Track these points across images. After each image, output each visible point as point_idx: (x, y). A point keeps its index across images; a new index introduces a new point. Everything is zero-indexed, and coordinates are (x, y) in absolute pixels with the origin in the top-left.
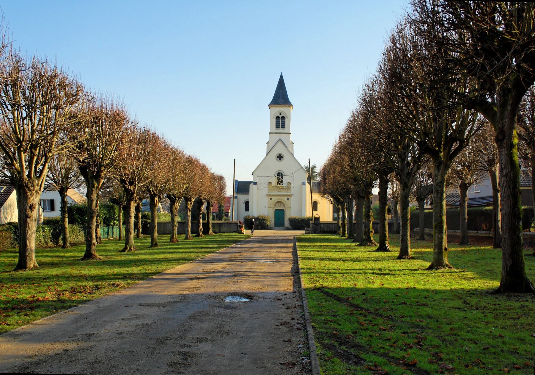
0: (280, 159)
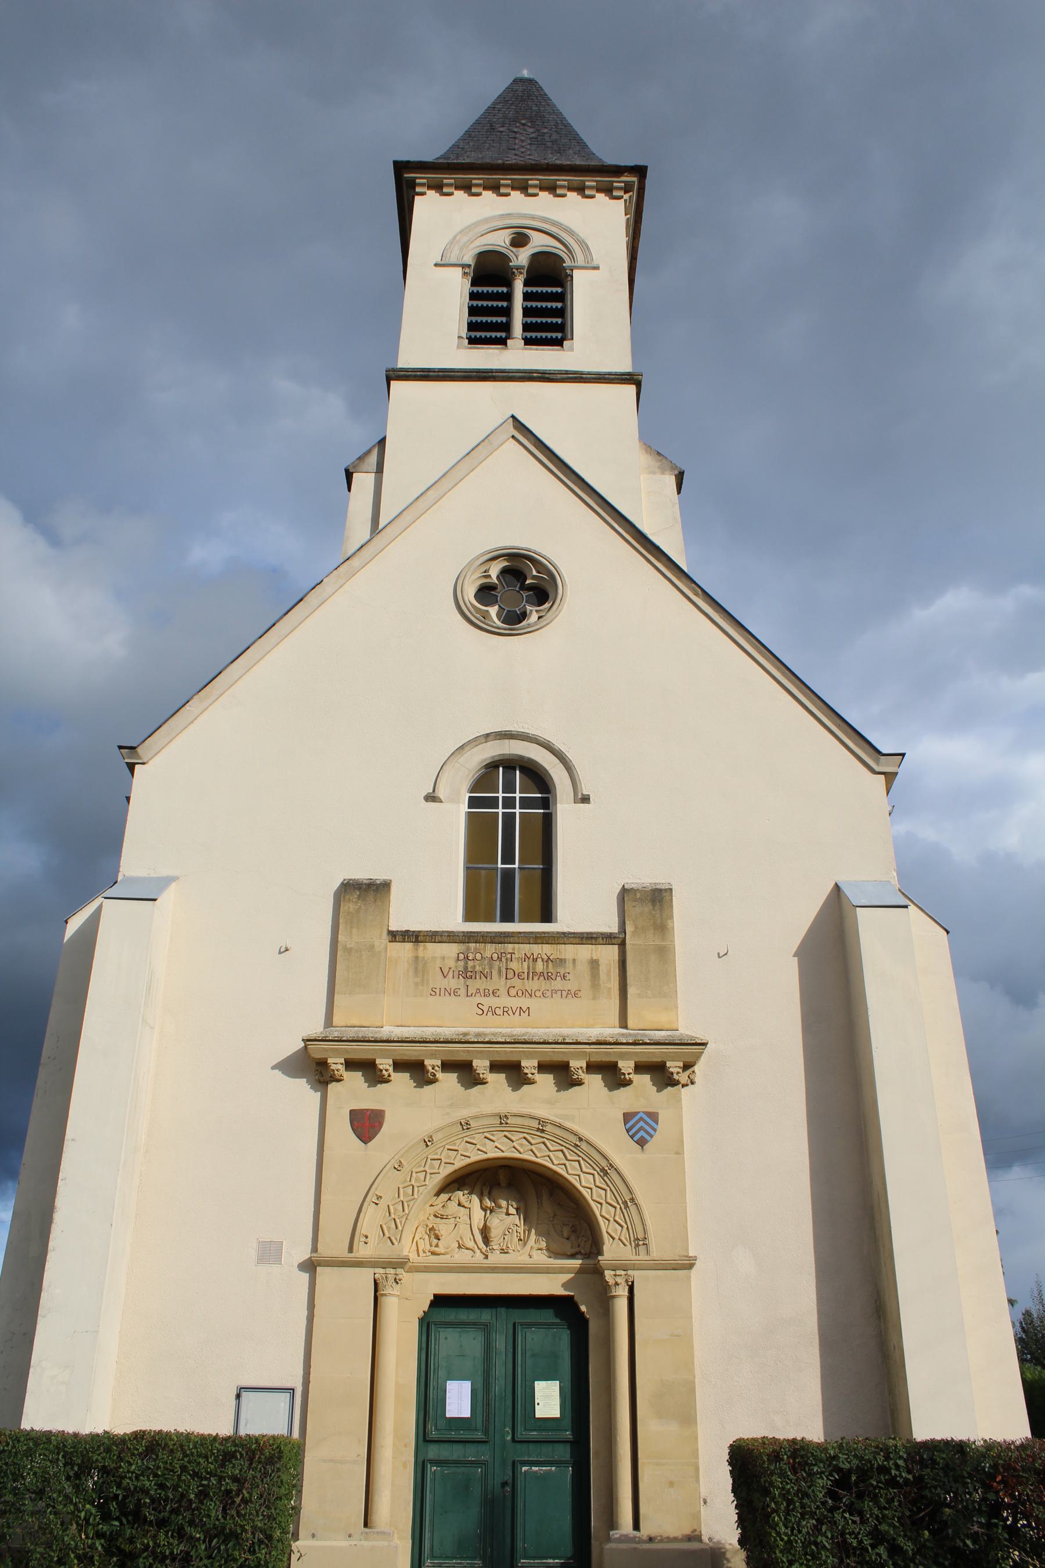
0: (514, 619)
